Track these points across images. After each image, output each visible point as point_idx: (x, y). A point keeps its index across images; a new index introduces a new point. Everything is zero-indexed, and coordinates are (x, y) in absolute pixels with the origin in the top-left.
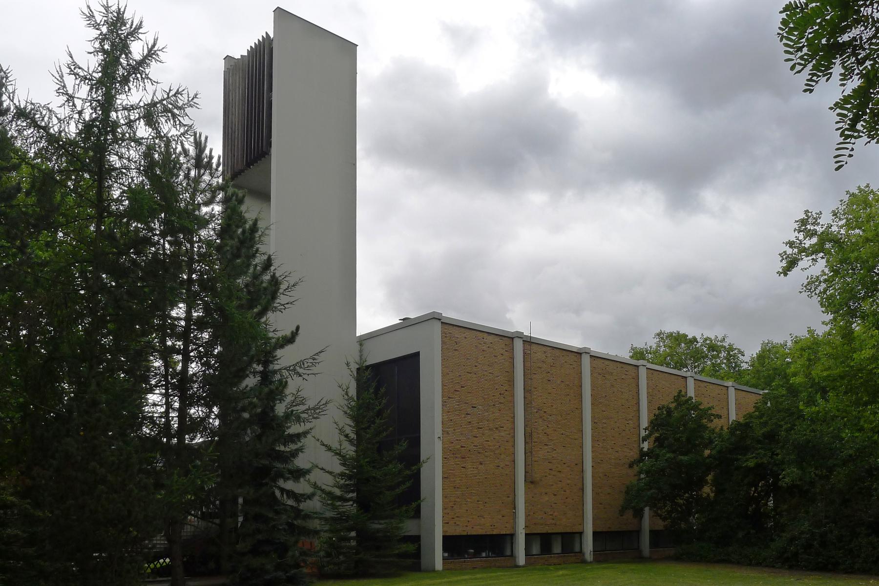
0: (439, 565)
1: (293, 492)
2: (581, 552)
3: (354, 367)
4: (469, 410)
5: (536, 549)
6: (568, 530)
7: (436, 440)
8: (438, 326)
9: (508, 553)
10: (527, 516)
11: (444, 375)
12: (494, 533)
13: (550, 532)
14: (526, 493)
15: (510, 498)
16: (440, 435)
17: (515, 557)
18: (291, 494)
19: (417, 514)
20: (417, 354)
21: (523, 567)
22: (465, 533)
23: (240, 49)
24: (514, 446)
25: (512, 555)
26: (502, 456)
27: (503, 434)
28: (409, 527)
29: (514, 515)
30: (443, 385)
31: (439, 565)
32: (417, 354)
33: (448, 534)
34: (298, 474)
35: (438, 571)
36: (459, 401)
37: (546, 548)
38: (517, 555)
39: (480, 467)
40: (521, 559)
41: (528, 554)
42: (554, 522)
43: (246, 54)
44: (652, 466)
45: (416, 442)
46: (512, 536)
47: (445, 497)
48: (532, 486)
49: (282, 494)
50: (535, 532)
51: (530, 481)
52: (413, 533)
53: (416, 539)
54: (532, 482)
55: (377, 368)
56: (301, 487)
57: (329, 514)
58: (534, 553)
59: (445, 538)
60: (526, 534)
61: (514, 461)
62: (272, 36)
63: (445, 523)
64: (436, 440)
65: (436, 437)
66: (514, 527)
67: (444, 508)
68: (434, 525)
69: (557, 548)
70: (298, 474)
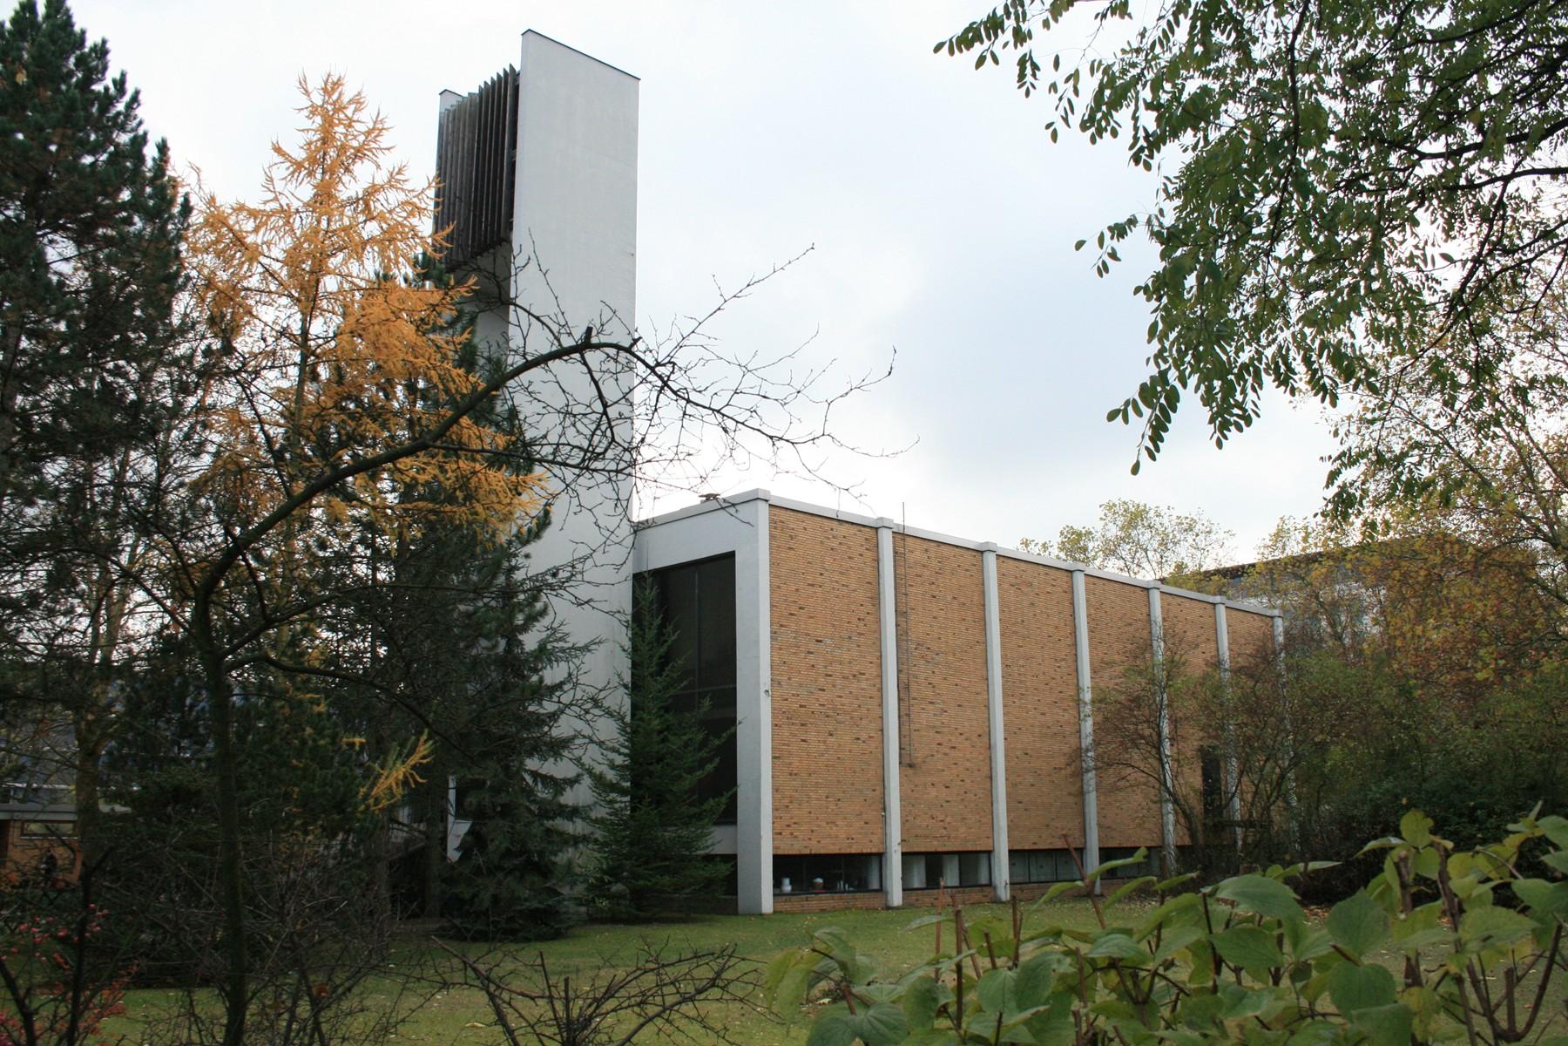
0: (767, 904)
1: (552, 778)
2: (990, 884)
3: (629, 570)
4: (812, 646)
5: (918, 880)
6: (970, 848)
7: (763, 694)
8: (763, 508)
9: (875, 885)
10: (904, 822)
11: (774, 589)
12: (853, 851)
13: (939, 849)
14: (901, 785)
15: (877, 793)
16: (768, 687)
17: (886, 893)
18: (548, 780)
19: (729, 816)
20: (731, 555)
21: (897, 908)
22: (807, 852)
23: (470, 83)
24: (881, 705)
25: (881, 890)
26: (864, 722)
27: (863, 685)
28: (718, 840)
29: (884, 820)
30: (772, 606)
31: (767, 904)
32: (731, 555)
33: (780, 852)
34: (557, 747)
35: (768, 915)
36: (796, 632)
37: (933, 879)
38: (889, 889)
39: (831, 740)
40: (896, 897)
41: (906, 889)
42: (945, 832)
43: (477, 91)
44: (1284, 546)
45: (728, 698)
46: (880, 857)
47: (776, 790)
48: (910, 771)
49: (535, 781)
50: (916, 850)
51: (907, 764)
52: (720, 849)
53: (732, 859)
54: (911, 766)
55: (664, 576)
56: (560, 768)
57: (601, 812)
58: (916, 886)
59: (776, 858)
60: (903, 854)
61: (882, 730)
62: (517, 69)
63: (777, 834)
64: (763, 694)
65: (763, 689)
66: (885, 836)
67: (775, 809)
68: (760, 837)
69: (951, 877)
70: (557, 747)
